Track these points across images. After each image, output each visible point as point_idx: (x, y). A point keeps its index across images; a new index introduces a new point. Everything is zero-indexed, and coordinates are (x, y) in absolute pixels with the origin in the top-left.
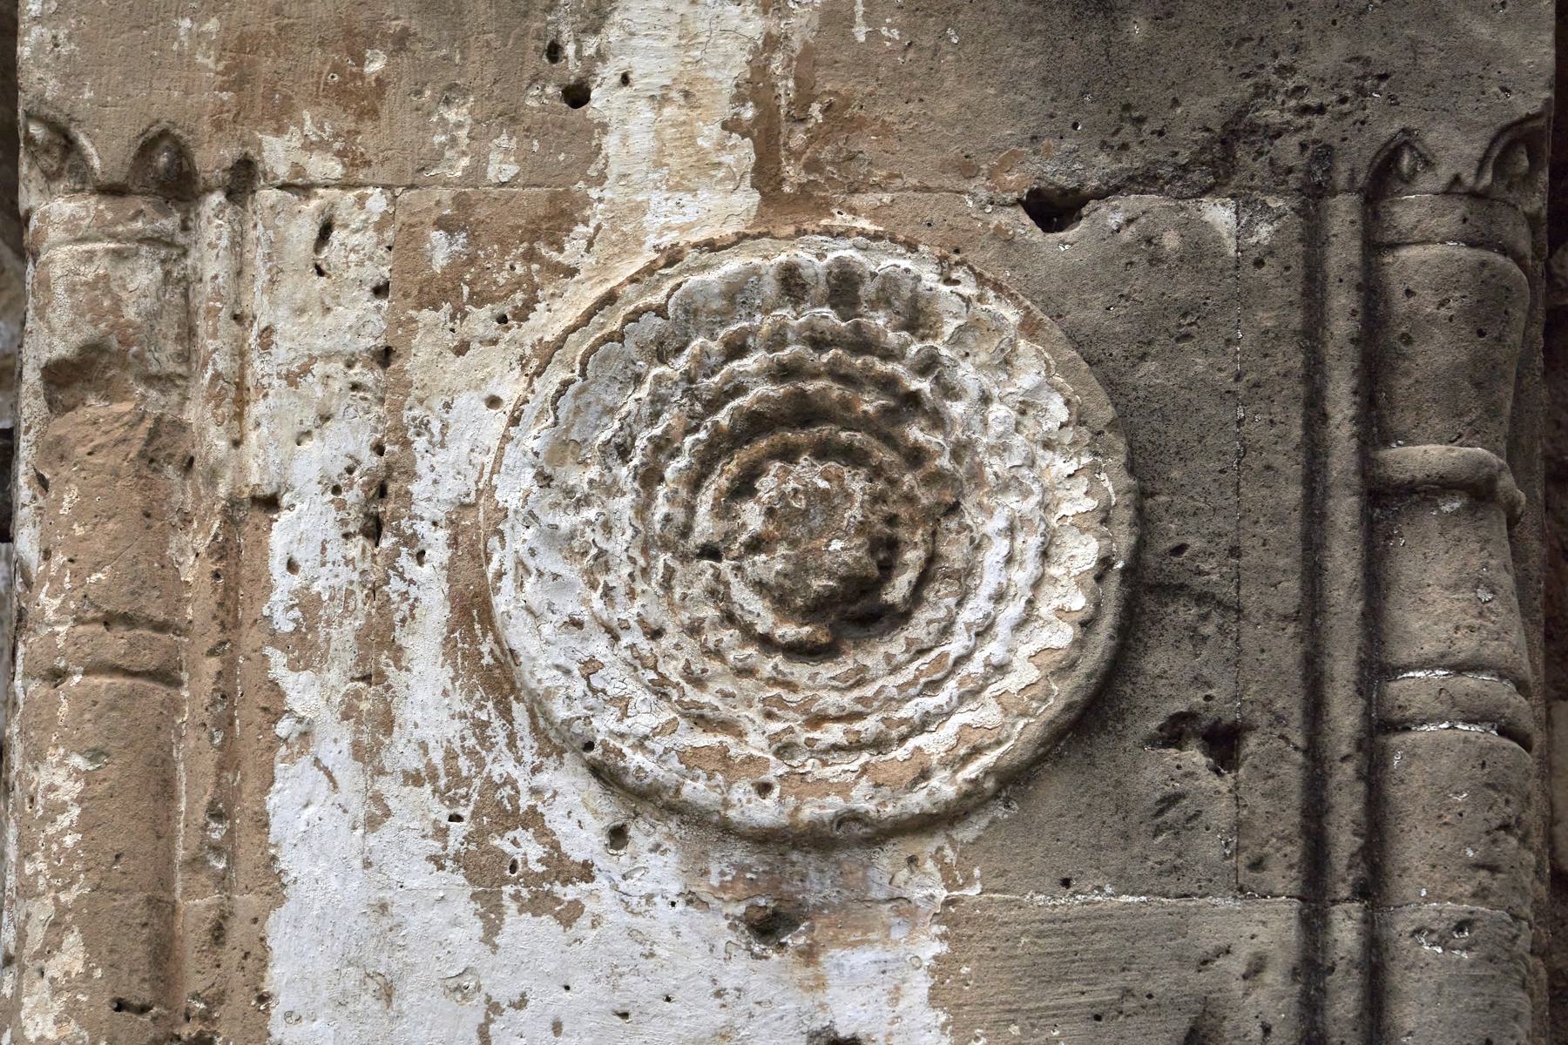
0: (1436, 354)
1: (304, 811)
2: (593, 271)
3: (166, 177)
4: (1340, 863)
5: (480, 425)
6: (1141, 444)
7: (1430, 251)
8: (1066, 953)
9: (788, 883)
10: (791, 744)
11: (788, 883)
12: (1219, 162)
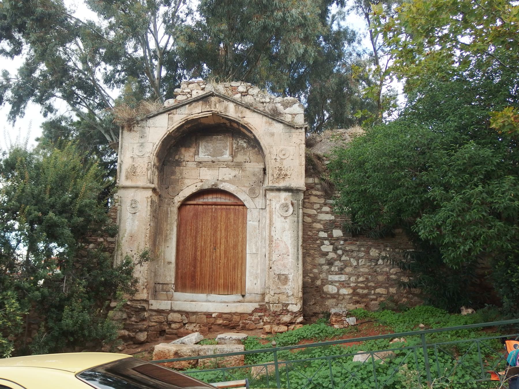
0: (300, 205)
1: (274, 216)
4: (298, 217)
5: (278, 206)
7: (300, 202)
9: (285, 218)
10: (285, 214)
11: (285, 218)
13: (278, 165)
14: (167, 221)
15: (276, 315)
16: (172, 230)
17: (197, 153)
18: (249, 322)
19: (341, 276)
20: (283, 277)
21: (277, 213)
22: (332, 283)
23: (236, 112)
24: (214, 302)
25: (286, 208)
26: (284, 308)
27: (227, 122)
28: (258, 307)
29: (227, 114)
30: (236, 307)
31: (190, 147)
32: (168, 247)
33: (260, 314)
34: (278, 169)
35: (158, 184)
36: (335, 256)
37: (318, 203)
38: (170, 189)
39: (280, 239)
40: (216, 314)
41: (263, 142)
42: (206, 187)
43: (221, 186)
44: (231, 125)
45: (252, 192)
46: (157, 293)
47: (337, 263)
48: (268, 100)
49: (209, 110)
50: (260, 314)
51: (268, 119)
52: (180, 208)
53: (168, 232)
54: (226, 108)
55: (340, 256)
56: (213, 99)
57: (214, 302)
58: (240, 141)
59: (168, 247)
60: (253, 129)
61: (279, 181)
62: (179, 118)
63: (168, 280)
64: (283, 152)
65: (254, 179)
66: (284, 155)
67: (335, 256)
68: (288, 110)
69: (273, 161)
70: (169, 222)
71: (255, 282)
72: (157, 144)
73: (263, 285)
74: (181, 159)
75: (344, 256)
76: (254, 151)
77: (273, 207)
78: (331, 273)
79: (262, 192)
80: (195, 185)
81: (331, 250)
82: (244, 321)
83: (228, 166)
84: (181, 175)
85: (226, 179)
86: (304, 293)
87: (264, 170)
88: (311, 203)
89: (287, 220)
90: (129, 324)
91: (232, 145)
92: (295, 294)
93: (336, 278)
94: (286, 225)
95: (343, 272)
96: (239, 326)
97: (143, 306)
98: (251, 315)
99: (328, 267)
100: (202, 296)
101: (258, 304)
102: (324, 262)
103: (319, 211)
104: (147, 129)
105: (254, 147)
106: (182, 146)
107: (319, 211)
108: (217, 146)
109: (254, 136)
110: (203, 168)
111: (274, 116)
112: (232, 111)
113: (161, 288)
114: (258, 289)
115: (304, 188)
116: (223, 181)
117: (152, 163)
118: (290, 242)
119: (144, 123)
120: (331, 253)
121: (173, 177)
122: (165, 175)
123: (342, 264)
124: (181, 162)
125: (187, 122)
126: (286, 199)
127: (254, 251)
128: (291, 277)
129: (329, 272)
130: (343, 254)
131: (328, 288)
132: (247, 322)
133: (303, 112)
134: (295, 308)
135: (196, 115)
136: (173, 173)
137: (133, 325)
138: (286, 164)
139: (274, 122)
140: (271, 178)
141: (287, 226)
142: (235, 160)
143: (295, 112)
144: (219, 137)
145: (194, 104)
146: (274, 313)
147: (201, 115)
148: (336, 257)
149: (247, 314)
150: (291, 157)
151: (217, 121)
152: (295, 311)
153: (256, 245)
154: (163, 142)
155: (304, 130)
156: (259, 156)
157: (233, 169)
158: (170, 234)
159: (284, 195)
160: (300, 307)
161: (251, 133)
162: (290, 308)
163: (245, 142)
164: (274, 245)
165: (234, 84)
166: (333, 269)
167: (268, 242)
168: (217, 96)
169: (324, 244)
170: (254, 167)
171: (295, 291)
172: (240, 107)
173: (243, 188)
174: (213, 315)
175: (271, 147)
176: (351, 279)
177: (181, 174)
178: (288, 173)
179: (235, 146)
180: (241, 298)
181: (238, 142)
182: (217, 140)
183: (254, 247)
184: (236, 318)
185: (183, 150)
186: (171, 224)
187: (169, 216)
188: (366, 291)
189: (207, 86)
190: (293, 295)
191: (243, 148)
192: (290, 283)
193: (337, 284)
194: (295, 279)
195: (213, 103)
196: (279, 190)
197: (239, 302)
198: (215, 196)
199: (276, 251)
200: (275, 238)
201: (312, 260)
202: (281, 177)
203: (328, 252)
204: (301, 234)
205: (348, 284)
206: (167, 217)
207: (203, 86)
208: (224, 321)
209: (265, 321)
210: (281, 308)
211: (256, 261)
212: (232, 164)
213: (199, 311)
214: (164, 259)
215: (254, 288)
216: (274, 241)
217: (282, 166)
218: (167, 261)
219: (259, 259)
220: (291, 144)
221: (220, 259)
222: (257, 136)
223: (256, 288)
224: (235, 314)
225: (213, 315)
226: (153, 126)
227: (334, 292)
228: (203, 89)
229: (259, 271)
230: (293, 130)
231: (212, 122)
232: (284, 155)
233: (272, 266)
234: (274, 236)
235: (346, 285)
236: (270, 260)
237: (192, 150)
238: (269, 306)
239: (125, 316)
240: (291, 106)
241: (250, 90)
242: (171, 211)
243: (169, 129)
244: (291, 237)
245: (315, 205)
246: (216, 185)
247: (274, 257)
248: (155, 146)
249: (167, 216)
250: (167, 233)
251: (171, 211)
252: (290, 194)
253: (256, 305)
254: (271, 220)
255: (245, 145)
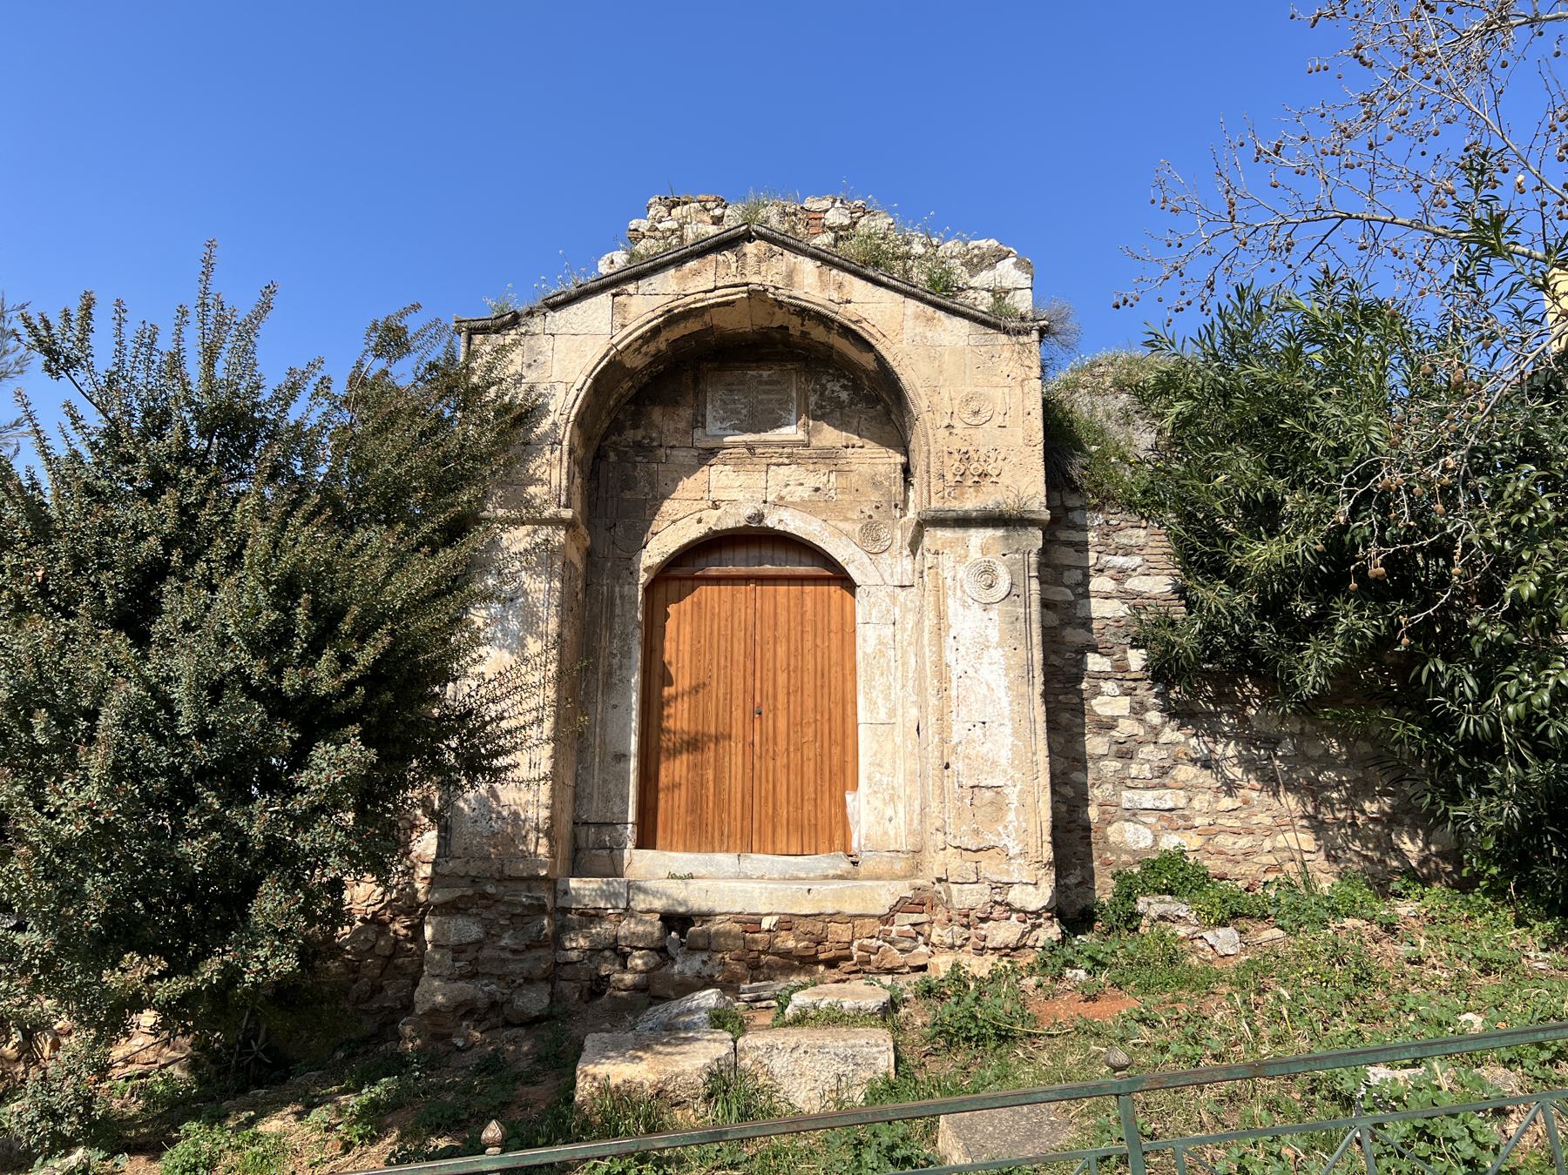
0: (1034, 566)
1: (950, 601)
2: (970, 560)
3: (937, 553)
4: (1027, 605)
5: (961, 572)
6: (1012, 574)
7: (1033, 559)
8: (1007, 612)
9: (986, 607)
10: (988, 596)
11: (986, 607)
12: (1017, 551)
13: (956, 444)
14: (611, 629)
15: (970, 920)
16: (626, 654)
17: (698, 422)
18: (880, 943)
19: (1162, 792)
20: (989, 794)
21: (959, 593)
22: (1133, 814)
23: (824, 286)
24: (762, 877)
25: (988, 578)
26: (998, 898)
27: (796, 321)
28: (910, 894)
29: (795, 293)
30: (838, 896)
31: (676, 404)
32: (615, 707)
33: (915, 918)
34: (957, 456)
35: (581, 513)
36: (1140, 731)
37: (1077, 568)
38: (620, 530)
39: (971, 672)
40: (776, 918)
41: (911, 376)
42: (729, 523)
43: (771, 521)
44: (804, 334)
45: (870, 532)
46: (580, 855)
47: (1146, 751)
48: (918, 249)
49: (738, 280)
50: (915, 918)
51: (921, 305)
52: (649, 589)
53: (616, 661)
54: (790, 276)
55: (1155, 731)
56: (750, 248)
57: (762, 877)
58: (829, 385)
59: (615, 707)
60: (878, 336)
61: (962, 494)
62: (648, 302)
63: (616, 810)
64: (974, 406)
65: (875, 497)
66: (976, 413)
67: (1140, 731)
68: (984, 278)
69: (943, 433)
70: (617, 629)
71: (889, 812)
72: (578, 386)
73: (916, 822)
74: (652, 440)
75: (1167, 730)
76: (872, 413)
77: (948, 574)
78: (1129, 783)
79: (900, 535)
80: (697, 516)
81: (1126, 712)
82: (866, 942)
83: (793, 460)
84: (652, 487)
85: (788, 498)
86: (1056, 844)
87: (906, 470)
88: (1055, 567)
89: (993, 614)
90: (491, 959)
91: (807, 398)
92: (1032, 852)
93: (1148, 799)
94: (989, 631)
95: (1167, 781)
96: (849, 958)
97: (538, 899)
98: (886, 919)
99: (1117, 764)
100: (725, 860)
101: (907, 883)
102: (1102, 750)
103: (1080, 590)
104: (544, 343)
105: (872, 401)
106: (653, 403)
107: (1080, 590)
108: (761, 402)
109: (880, 360)
110: (721, 467)
111: (941, 296)
112: (810, 284)
113: (592, 837)
114: (899, 834)
115: (1046, 515)
116: (781, 503)
117: (565, 443)
118: (1004, 682)
119: (536, 324)
120: (1128, 722)
121: (627, 495)
122: (602, 490)
123: (1164, 754)
124: (651, 449)
125: (672, 319)
126: (984, 550)
127: (882, 715)
128: (1012, 795)
129: (1123, 782)
130: (1164, 724)
131: (1121, 832)
132: (875, 943)
133: (1028, 283)
134: (1038, 896)
135: (699, 296)
136: (628, 483)
137: (504, 961)
138: (984, 439)
139: (941, 314)
140: (936, 485)
141: (994, 635)
142: (814, 442)
143: (1007, 284)
144: (765, 374)
145: (692, 264)
146: (967, 916)
147: (713, 299)
148: (1142, 732)
149: (873, 916)
150: (998, 420)
151: (761, 320)
152: (1032, 908)
153: (887, 698)
154: (596, 380)
155: (1035, 335)
156: (888, 428)
157: (811, 467)
158: (620, 667)
159: (978, 537)
160: (1049, 893)
161: (870, 347)
162: (1016, 896)
163: (844, 387)
164: (954, 693)
165: (811, 204)
166: (1134, 773)
167: (932, 684)
168: (762, 237)
169: (1100, 693)
170: (876, 460)
171: (1032, 841)
172: (835, 272)
173: (841, 525)
174: (767, 923)
175: (935, 389)
176: (1196, 804)
177: (652, 485)
178: (989, 470)
179: (813, 399)
180: (845, 865)
181: (824, 387)
182: (760, 383)
183: (880, 702)
184: (840, 932)
185: (657, 414)
186: (625, 637)
187: (618, 611)
188: (1244, 842)
189: (728, 212)
190: (1024, 854)
191: (840, 405)
192: (1011, 816)
193: (1151, 820)
194: (1029, 800)
195: (751, 260)
196: (964, 521)
197: (841, 877)
198: (754, 552)
199: (963, 711)
200: (957, 670)
201: (1067, 742)
202: (970, 483)
203: (1115, 719)
204: (1038, 656)
205: (1185, 818)
206: (612, 616)
207: (718, 212)
208: (798, 941)
209: (934, 939)
210: (987, 898)
211: (889, 747)
212: (807, 452)
213: (718, 910)
214: (603, 742)
215: (886, 833)
216: (954, 678)
217: (971, 449)
218: (611, 749)
219: (898, 740)
220: (997, 379)
221: (775, 743)
222: (889, 358)
223: (892, 833)
224: (834, 917)
225: (767, 923)
226: (564, 330)
227: (1142, 845)
228: (717, 221)
229: (900, 780)
230: (1003, 338)
231: (746, 326)
232: (976, 413)
233: (952, 760)
234: (953, 663)
235: (1181, 823)
236: (943, 741)
237: (686, 413)
238: (948, 892)
239: (474, 931)
240: (991, 266)
241: (863, 221)
242: (622, 597)
243: (615, 341)
244: (1008, 668)
245: (1066, 574)
246: (760, 517)
247: (958, 732)
248: (573, 393)
249: (612, 612)
250: (610, 665)
251: (622, 597)
252: (1000, 532)
253: (903, 889)
254: (940, 617)
255: (844, 396)
